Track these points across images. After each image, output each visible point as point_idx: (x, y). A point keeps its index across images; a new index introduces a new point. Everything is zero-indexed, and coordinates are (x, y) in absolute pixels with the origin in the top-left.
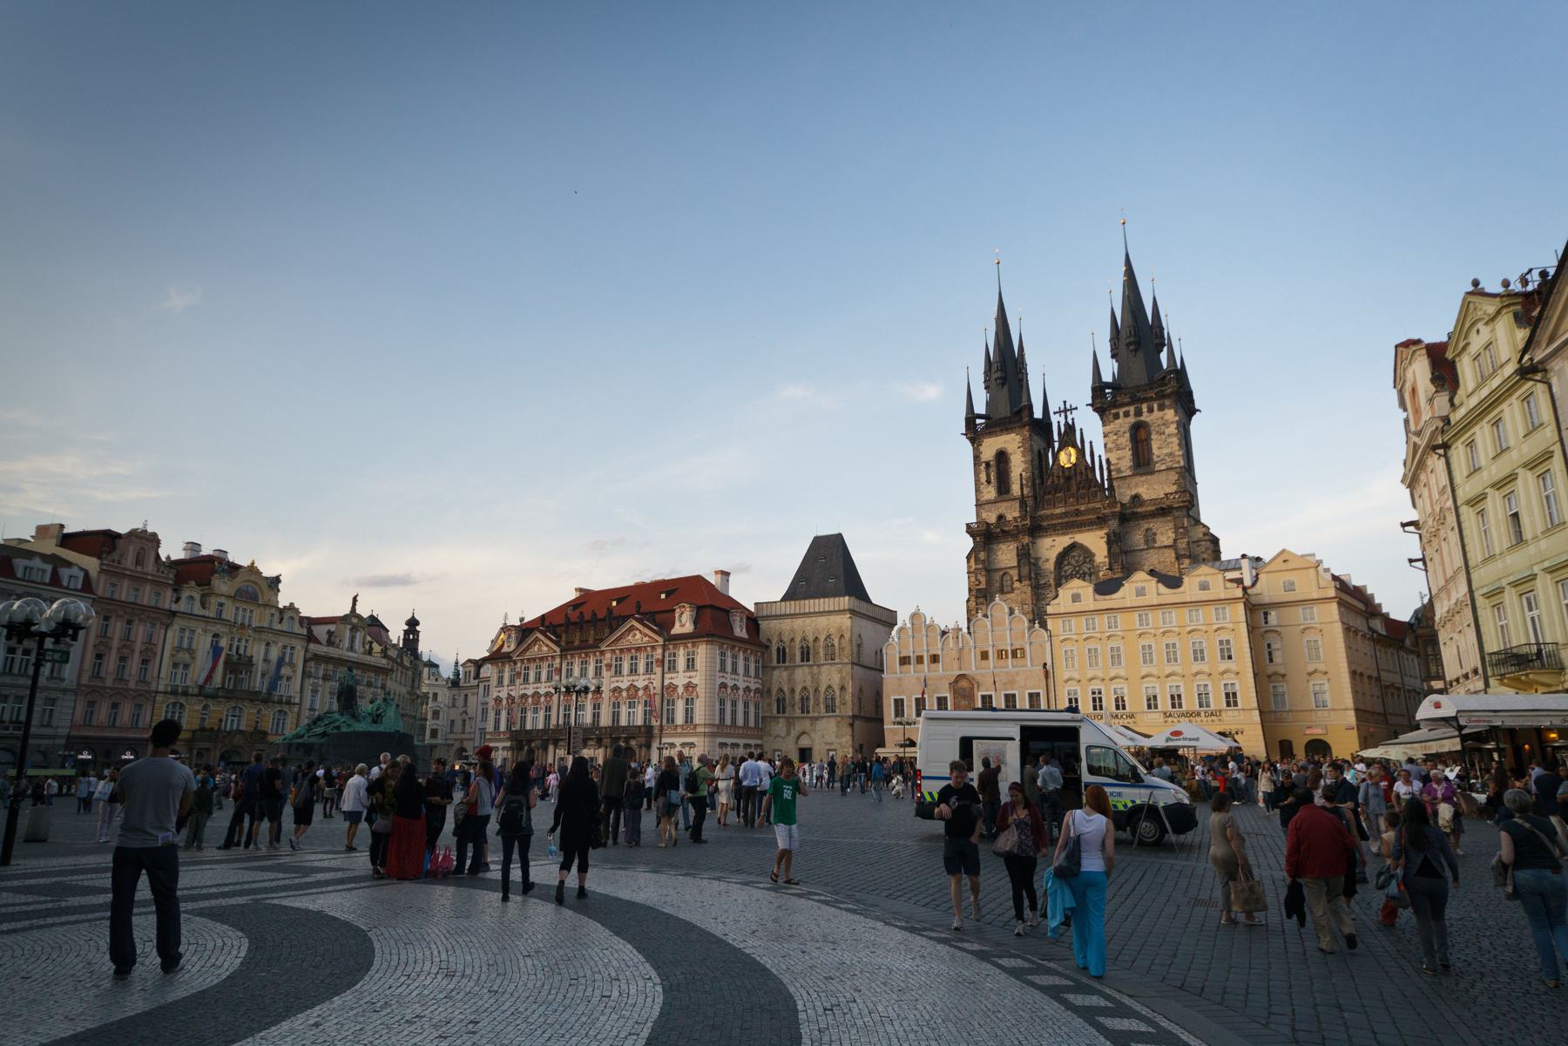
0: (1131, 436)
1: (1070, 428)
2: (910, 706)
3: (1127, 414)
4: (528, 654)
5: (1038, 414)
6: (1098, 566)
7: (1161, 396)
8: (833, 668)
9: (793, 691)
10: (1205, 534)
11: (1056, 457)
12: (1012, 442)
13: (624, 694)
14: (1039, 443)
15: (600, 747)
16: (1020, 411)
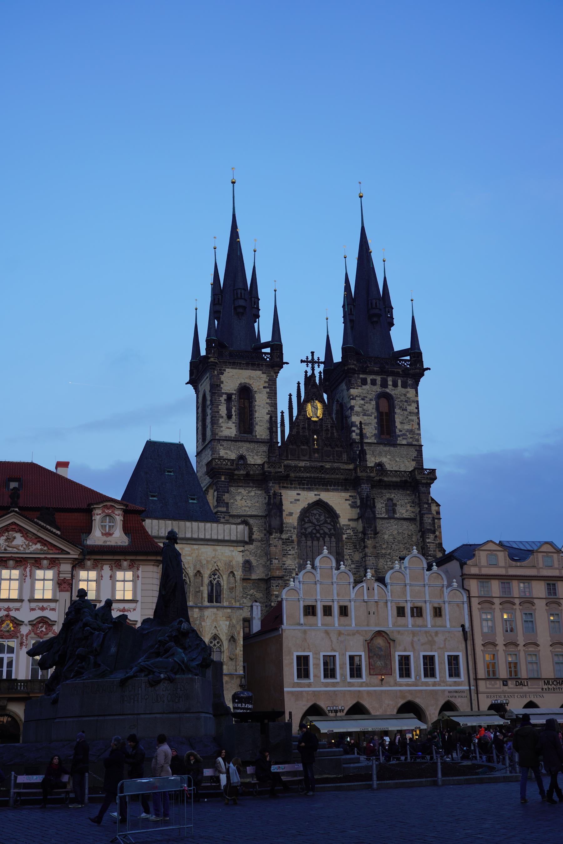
2: (317, 665)
3: (374, 383)
8: (220, 613)
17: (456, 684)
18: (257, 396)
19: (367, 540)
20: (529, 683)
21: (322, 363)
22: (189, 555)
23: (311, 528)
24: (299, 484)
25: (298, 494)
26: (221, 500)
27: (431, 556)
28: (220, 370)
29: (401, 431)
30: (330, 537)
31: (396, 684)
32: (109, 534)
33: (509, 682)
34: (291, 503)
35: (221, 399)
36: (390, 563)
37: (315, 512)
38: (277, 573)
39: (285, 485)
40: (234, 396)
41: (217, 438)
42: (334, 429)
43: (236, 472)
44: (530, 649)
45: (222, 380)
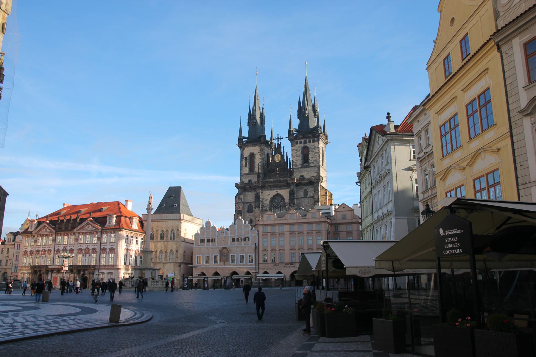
0: (302, 151)
1: (279, 146)
2: (203, 259)
3: (301, 143)
4: (40, 232)
5: (268, 138)
6: (286, 204)
7: (314, 136)
8: (173, 243)
9: (156, 252)
11: (273, 158)
12: (255, 149)
13: (83, 251)
14: (267, 150)
15: (72, 273)
16: (260, 137)
17: (251, 265)
18: (256, 156)
19: (291, 207)
20: (279, 264)
21: (275, 139)
22: (164, 225)
23: (276, 204)
24: (270, 188)
25: (270, 192)
29: (311, 161)
30: (283, 207)
31: (230, 265)
32: (110, 224)
35: (243, 159)
37: (277, 198)
39: (265, 189)
40: (248, 158)
41: (242, 174)
43: (246, 187)
44: (281, 252)
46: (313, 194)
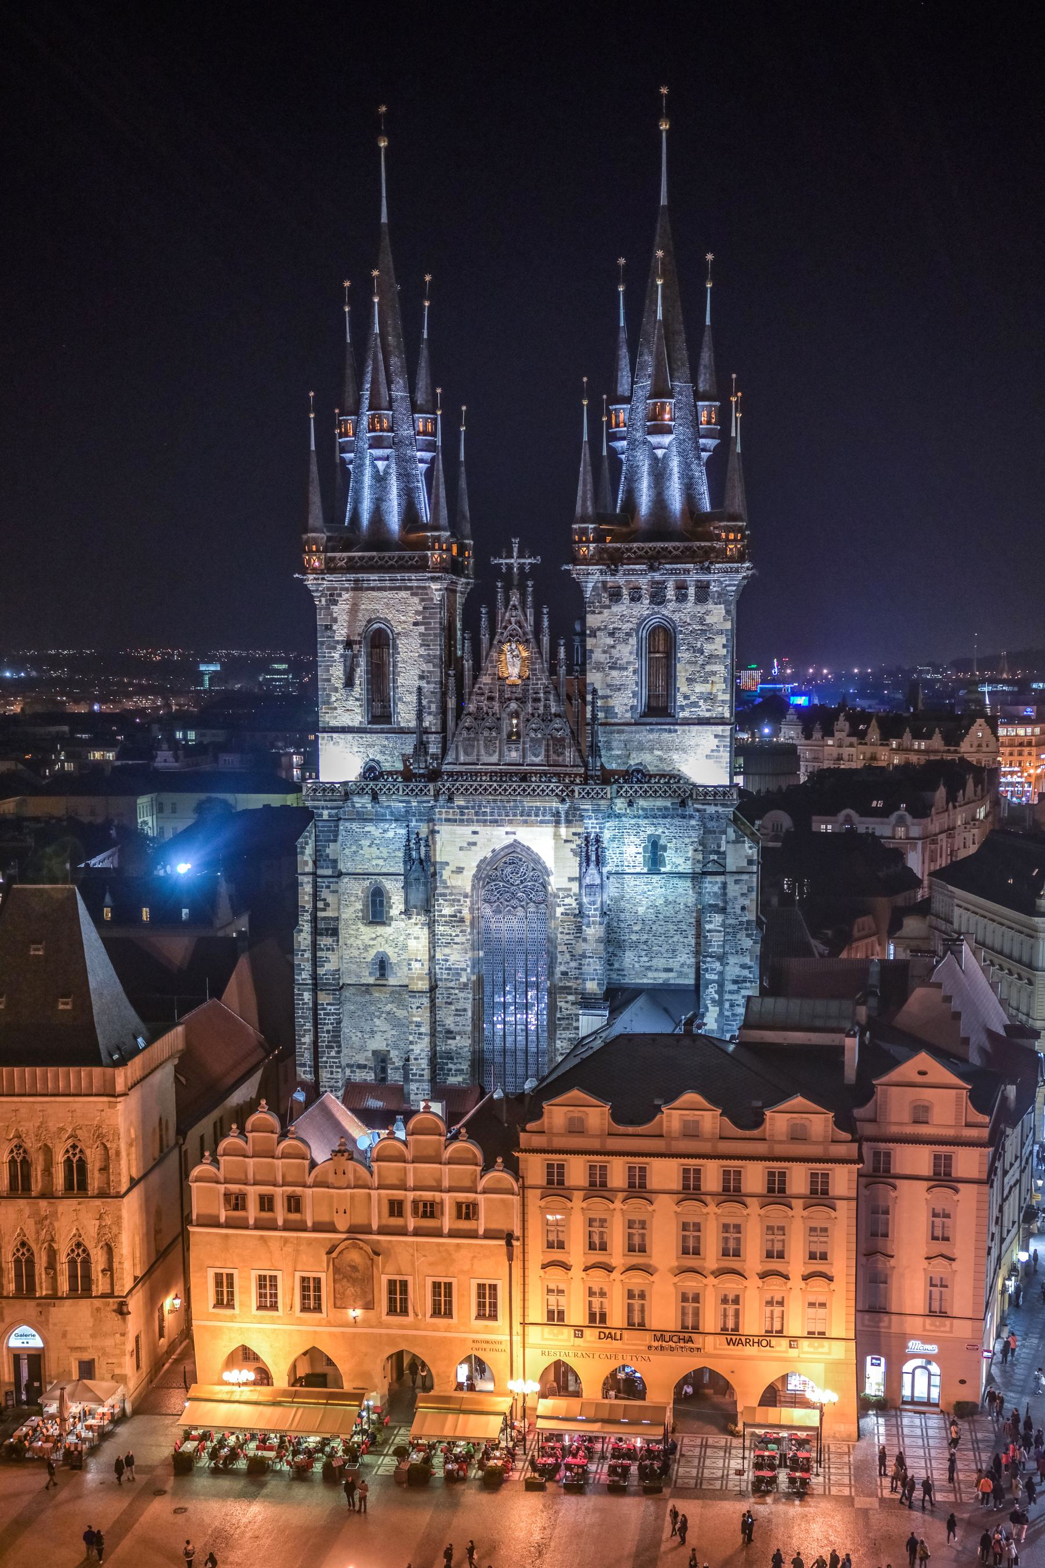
0: (640, 641)
3: (635, 598)
6: (556, 896)
10: (750, 862)
17: (487, 1330)
18: (401, 643)
19: (588, 926)
24: (477, 814)
25: (475, 833)
26: (321, 855)
27: (712, 957)
28: (331, 595)
29: (686, 697)
31: (380, 1324)
33: (587, 1332)
34: (461, 849)
36: (646, 959)
38: (420, 986)
39: (450, 817)
42: (552, 697)
45: (335, 615)
46: (688, 859)
